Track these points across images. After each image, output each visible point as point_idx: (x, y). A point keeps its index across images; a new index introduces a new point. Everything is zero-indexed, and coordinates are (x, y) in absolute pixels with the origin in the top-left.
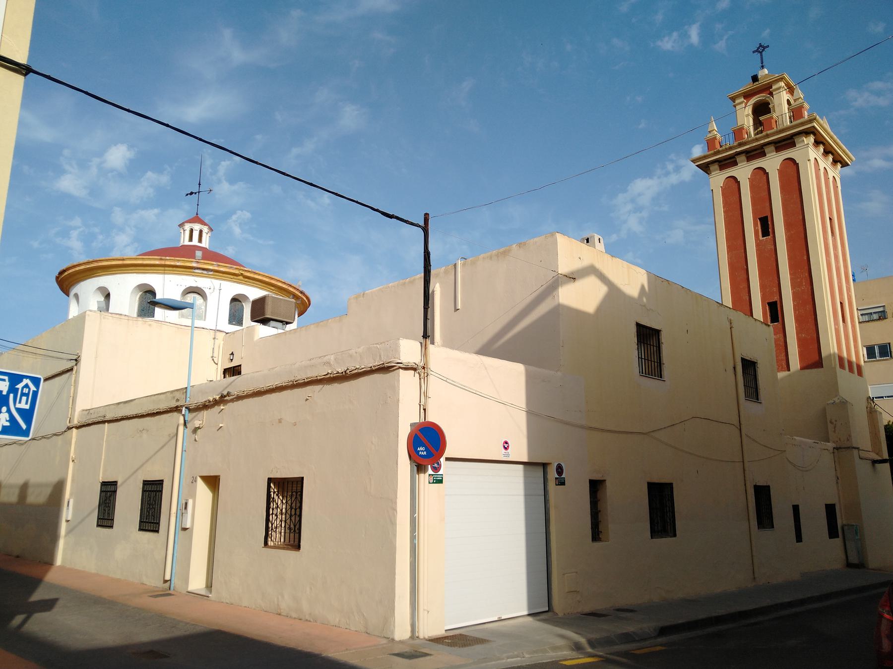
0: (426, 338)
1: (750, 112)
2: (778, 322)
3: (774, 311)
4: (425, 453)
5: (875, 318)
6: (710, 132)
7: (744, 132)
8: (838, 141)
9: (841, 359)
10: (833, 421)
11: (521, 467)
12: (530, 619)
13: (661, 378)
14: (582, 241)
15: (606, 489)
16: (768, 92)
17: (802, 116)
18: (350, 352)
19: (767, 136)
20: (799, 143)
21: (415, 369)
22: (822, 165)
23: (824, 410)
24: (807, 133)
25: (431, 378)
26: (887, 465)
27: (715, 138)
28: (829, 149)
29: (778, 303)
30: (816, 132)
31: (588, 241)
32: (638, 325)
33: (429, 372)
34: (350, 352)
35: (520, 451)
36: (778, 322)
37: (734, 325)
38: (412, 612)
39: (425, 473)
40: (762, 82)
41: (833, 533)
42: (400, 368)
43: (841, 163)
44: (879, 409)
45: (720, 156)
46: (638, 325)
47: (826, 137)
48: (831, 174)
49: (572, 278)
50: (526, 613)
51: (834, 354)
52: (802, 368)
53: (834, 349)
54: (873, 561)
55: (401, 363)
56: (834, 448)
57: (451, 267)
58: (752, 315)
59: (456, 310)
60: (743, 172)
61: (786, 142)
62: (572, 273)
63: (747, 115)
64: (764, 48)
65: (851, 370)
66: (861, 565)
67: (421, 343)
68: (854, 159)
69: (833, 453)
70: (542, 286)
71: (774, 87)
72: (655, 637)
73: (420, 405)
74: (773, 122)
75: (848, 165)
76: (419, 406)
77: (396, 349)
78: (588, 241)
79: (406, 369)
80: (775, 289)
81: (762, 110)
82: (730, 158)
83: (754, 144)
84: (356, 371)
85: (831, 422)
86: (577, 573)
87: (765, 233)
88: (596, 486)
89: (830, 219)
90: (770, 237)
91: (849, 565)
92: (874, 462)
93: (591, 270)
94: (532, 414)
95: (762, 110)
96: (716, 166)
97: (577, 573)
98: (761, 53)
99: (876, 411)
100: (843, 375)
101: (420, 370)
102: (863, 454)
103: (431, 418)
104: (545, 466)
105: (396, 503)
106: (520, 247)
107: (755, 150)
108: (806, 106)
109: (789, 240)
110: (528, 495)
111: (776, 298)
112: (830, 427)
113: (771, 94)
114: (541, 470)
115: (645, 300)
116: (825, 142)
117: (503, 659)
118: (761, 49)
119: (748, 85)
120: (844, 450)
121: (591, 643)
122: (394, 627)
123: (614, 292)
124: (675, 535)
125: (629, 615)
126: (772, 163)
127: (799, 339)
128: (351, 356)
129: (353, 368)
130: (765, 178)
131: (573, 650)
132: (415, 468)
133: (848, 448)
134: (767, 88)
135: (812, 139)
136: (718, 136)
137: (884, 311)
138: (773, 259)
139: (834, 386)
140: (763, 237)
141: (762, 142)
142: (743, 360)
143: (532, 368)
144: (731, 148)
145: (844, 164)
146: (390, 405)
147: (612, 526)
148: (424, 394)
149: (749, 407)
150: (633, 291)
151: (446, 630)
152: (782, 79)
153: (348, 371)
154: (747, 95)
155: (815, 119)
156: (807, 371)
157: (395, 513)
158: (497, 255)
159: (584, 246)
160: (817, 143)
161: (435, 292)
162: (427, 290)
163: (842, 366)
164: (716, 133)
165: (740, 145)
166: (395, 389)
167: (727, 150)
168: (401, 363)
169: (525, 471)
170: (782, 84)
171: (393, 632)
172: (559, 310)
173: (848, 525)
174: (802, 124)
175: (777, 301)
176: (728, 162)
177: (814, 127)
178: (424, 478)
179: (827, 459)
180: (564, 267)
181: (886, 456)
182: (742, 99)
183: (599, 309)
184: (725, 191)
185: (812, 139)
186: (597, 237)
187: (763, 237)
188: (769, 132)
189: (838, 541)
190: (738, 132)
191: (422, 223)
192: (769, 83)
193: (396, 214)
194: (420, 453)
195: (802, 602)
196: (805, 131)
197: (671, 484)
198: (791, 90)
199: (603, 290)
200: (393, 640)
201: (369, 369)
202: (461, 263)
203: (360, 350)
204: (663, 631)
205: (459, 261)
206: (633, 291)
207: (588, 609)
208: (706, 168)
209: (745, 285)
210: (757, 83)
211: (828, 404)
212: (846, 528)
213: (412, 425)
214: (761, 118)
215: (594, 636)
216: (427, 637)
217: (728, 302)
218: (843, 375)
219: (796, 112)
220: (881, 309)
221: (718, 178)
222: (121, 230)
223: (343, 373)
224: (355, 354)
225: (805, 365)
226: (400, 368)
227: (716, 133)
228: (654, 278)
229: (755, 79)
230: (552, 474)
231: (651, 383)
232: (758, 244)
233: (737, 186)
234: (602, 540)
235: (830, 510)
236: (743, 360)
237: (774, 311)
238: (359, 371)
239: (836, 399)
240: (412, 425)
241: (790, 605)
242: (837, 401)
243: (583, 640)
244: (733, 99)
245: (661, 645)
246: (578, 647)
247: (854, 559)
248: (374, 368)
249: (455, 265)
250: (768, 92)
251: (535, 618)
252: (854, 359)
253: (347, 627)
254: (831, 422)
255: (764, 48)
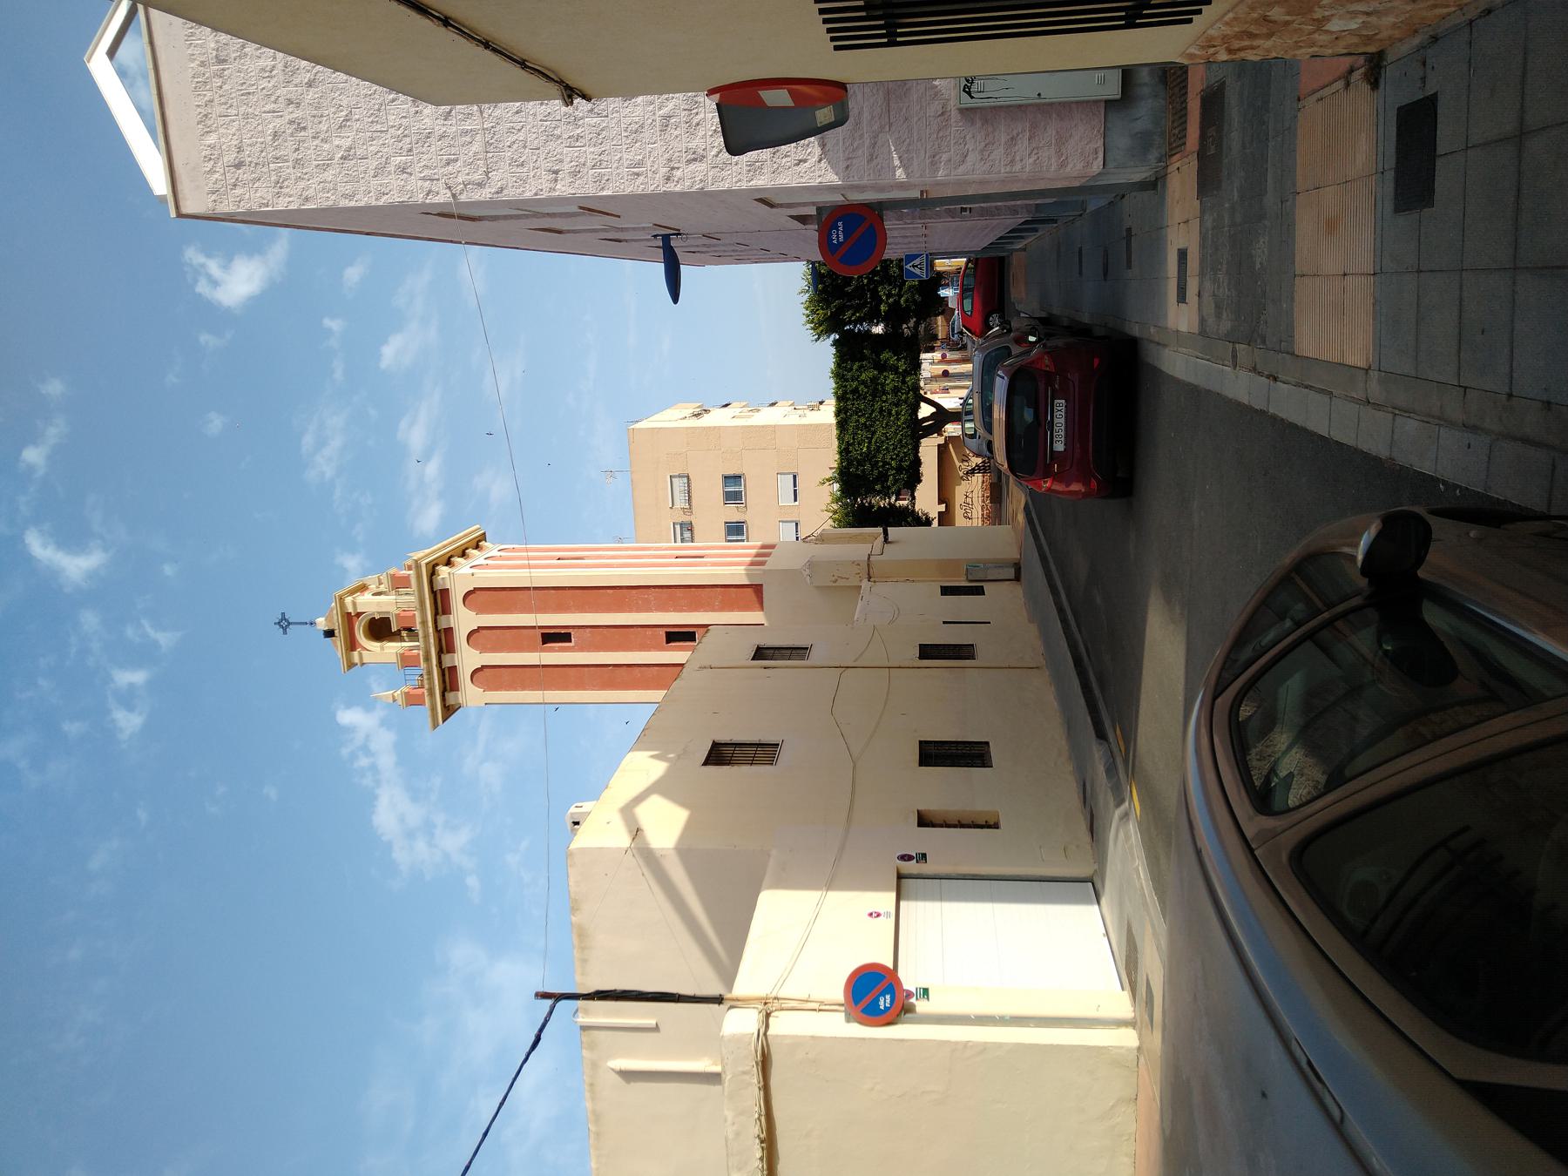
0: (722, 999)
1: (378, 644)
2: (694, 633)
3: (679, 636)
4: (888, 997)
5: (689, 535)
6: (394, 700)
7: (407, 653)
8: (451, 539)
9: (752, 564)
10: (834, 579)
11: (902, 904)
12: (1103, 901)
13: (778, 745)
14: (574, 832)
15: (929, 811)
16: (355, 618)
17: (407, 578)
18: (731, 1136)
19: (424, 623)
20: (444, 583)
21: (768, 1015)
22: (481, 561)
23: (817, 587)
24: (433, 573)
25: (781, 995)
26: (890, 529)
27: (407, 694)
28: (474, 543)
29: (668, 630)
30: (435, 562)
31: (577, 823)
32: (706, 763)
33: (774, 995)
34: (731, 1136)
35: (885, 900)
36: (694, 633)
37: (707, 663)
38: (1102, 1025)
39: (915, 1006)
40: (338, 625)
41: (979, 591)
42: (765, 1034)
43: (480, 541)
44: (819, 531)
45: (437, 687)
46: (706, 763)
47: (429, 559)
48: (495, 553)
49: (637, 832)
50: (1096, 907)
51: (746, 570)
52: (762, 608)
53: (741, 570)
54: (1014, 554)
55: (759, 1031)
56: (869, 581)
57: (586, 1037)
58: (682, 665)
59: (656, 1029)
60: (467, 659)
61: (440, 601)
62: (630, 832)
63: (382, 648)
64: (283, 618)
65: (768, 555)
66: (1017, 567)
67: (732, 1007)
68: (478, 526)
69: (875, 582)
70: (643, 875)
71: (350, 610)
72: (1109, 743)
73: (820, 1010)
74: (403, 614)
75: (484, 534)
76: (821, 1012)
77: (738, 1040)
78: (577, 823)
79: (767, 1026)
80: (649, 632)
81: (380, 629)
82: (443, 675)
83: (432, 641)
84: (763, 1119)
85: (835, 581)
86: (1040, 847)
87: (566, 638)
88: (924, 821)
89: (559, 559)
90: (572, 633)
91: (1017, 578)
92: (886, 540)
93: (628, 812)
94: (830, 885)
95: (380, 629)
96: (450, 696)
97: (1040, 847)
98: (289, 624)
99: (821, 535)
100: (772, 563)
101: (768, 1008)
102: (877, 550)
103: (840, 996)
104: (900, 877)
105: (956, 1043)
106: (577, 910)
107: (440, 640)
108: (392, 571)
109: (582, 608)
110: (941, 897)
111: (662, 632)
112: (841, 583)
113: (359, 615)
114: (904, 881)
115: (671, 756)
116: (449, 555)
117: (1141, 884)
118: (284, 624)
119: (338, 644)
120: (871, 570)
121: (1118, 805)
122: (1122, 1047)
123: (658, 788)
124: (987, 743)
125: (1088, 788)
126: (463, 620)
127: (722, 609)
128: (738, 1134)
129: (758, 1127)
130: (484, 631)
131: (1128, 820)
132: (908, 1015)
133: (868, 565)
134: (349, 619)
135: (443, 571)
136: (405, 689)
137: (681, 525)
138: (605, 630)
139: (788, 575)
140: (571, 642)
141: (431, 630)
142: (753, 659)
143: (766, 882)
144: (430, 673)
145: (483, 537)
146: (817, 1049)
147: (980, 805)
148: (803, 1005)
149: (815, 657)
150: (658, 769)
151: (1123, 989)
152: (341, 599)
153: (762, 1136)
154: (352, 645)
155: (416, 561)
156: (765, 604)
157: (970, 1044)
158: (583, 949)
159: (581, 829)
160: (448, 563)
161: (623, 1068)
162: (650, 996)
163: (763, 563)
164: (399, 692)
165: (427, 658)
166: (797, 1043)
167: (430, 679)
168: (759, 1031)
169: (908, 898)
170: (348, 600)
171: (1129, 1050)
172: (684, 850)
173: (967, 575)
174: (419, 576)
175: (666, 632)
176: (449, 679)
177: (427, 564)
178: (921, 1006)
179: (880, 588)
180: (623, 840)
181: (880, 530)
182: (356, 654)
183: (683, 804)
184: (489, 686)
185: (443, 571)
186: (573, 810)
187: (571, 642)
188: (418, 620)
189: (987, 587)
190: (406, 661)
191: (549, 1002)
192: (342, 616)
193: (536, 1031)
194: (888, 1005)
195: (1061, 610)
196: (429, 575)
197: (921, 742)
198: (363, 588)
199: (656, 800)
200: (1139, 1049)
201: (762, 1093)
202: (583, 1018)
203: (729, 1114)
204: (1101, 735)
205: (578, 1020)
206: (658, 769)
207: (1088, 838)
208: (449, 710)
209: (637, 670)
210: (336, 632)
211: (812, 583)
212: (970, 578)
213: (848, 1021)
214: (394, 629)
215: (1112, 803)
216: (1133, 1009)
217: (658, 695)
218: (772, 563)
219: (398, 584)
220: (678, 527)
221: (470, 694)
222: (870, 502)
223: (763, 1148)
224: (735, 1128)
225: (757, 605)
226: (765, 1034)
227: (399, 692)
228: (642, 743)
229: (330, 634)
230: (911, 867)
231: (785, 755)
232: (581, 649)
233: (488, 670)
234: (996, 821)
235: (946, 591)
236: (753, 659)
237: (679, 636)
238: (763, 1112)
239: (805, 573)
240: (848, 1021)
241: (1064, 621)
242: (808, 571)
243: (1118, 813)
244: (351, 665)
245: (1115, 731)
246: (1126, 815)
247: (1011, 573)
248: (762, 1083)
249: (584, 1028)
250: (355, 618)
251: (1101, 894)
252: (754, 551)
253: (1133, 1138)
254: (835, 581)
255: (283, 618)
